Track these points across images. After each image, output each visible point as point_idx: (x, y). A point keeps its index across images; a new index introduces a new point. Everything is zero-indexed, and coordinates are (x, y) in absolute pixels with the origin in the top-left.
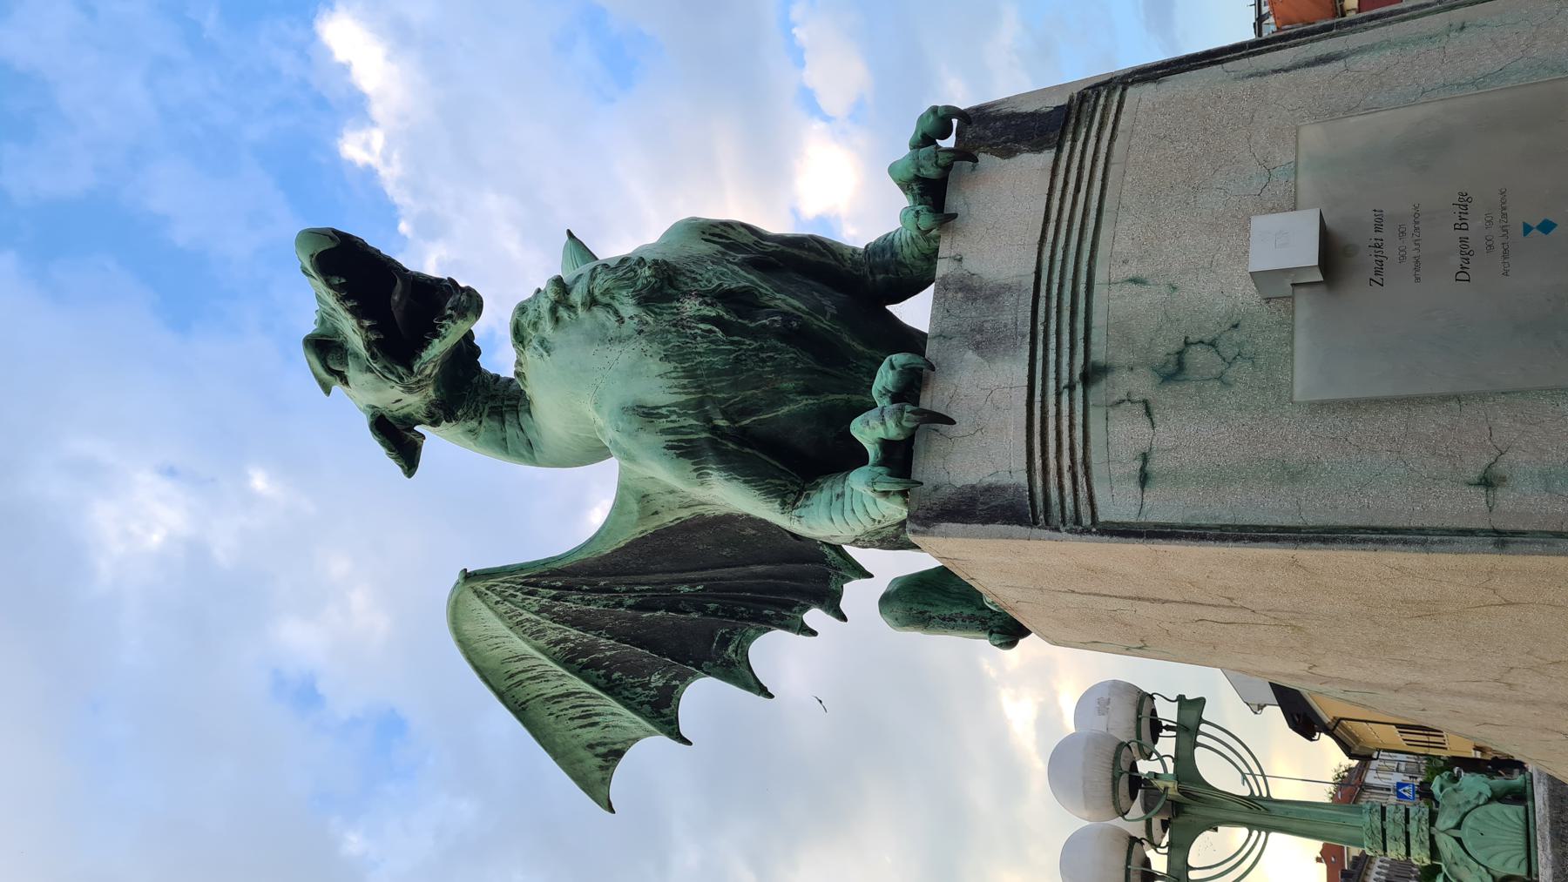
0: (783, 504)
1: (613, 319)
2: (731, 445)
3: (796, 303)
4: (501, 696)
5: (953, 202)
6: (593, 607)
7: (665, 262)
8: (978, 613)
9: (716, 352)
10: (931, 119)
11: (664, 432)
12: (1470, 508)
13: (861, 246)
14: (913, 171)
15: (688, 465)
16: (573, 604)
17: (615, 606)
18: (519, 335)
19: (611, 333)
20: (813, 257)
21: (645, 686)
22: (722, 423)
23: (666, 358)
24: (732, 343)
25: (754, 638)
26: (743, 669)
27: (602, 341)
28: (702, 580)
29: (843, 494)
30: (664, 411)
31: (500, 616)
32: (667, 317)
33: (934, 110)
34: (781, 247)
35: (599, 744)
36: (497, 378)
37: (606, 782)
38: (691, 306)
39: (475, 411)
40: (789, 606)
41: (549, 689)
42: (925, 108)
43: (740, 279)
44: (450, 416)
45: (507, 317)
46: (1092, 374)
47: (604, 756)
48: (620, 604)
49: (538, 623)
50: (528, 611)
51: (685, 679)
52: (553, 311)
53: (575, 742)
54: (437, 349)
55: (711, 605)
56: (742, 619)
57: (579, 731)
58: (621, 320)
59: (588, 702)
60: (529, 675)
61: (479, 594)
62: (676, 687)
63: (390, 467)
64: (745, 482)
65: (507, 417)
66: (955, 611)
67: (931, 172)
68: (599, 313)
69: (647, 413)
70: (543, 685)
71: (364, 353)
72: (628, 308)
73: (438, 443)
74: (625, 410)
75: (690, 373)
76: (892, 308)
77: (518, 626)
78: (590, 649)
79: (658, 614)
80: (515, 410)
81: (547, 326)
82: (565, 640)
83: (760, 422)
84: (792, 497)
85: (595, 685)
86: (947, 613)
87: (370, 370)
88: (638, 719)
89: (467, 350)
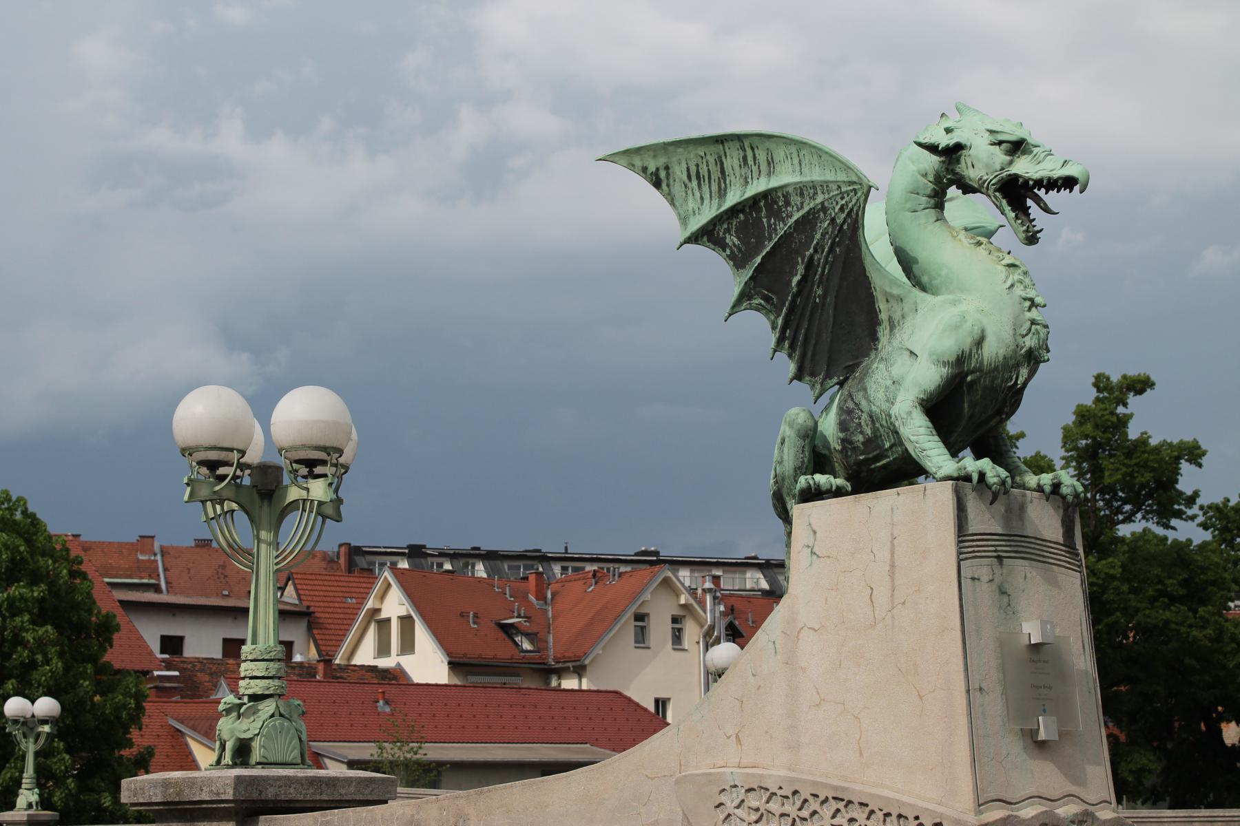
0: (922, 400)
4: (739, 138)
12: (974, 685)
15: (953, 359)
21: (728, 231)
22: (969, 378)
23: (1005, 358)
28: (823, 304)
37: (631, 166)
40: (792, 347)
46: (999, 558)
47: (656, 173)
48: (816, 251)
51: (738, 262)
52: (1032, 300)
59: (715, 187)
61: (851, 183)
62: (724, 251)
65: (933, 201)
69: (979, 342)
70: (736, 163)
73: (932, 162)
74: (983, 331)
75: (996, 368)
78: (775, 213)
79: (801, 269)
81: (1019, 291)
82: (787, 203)
87: (1002, 169)
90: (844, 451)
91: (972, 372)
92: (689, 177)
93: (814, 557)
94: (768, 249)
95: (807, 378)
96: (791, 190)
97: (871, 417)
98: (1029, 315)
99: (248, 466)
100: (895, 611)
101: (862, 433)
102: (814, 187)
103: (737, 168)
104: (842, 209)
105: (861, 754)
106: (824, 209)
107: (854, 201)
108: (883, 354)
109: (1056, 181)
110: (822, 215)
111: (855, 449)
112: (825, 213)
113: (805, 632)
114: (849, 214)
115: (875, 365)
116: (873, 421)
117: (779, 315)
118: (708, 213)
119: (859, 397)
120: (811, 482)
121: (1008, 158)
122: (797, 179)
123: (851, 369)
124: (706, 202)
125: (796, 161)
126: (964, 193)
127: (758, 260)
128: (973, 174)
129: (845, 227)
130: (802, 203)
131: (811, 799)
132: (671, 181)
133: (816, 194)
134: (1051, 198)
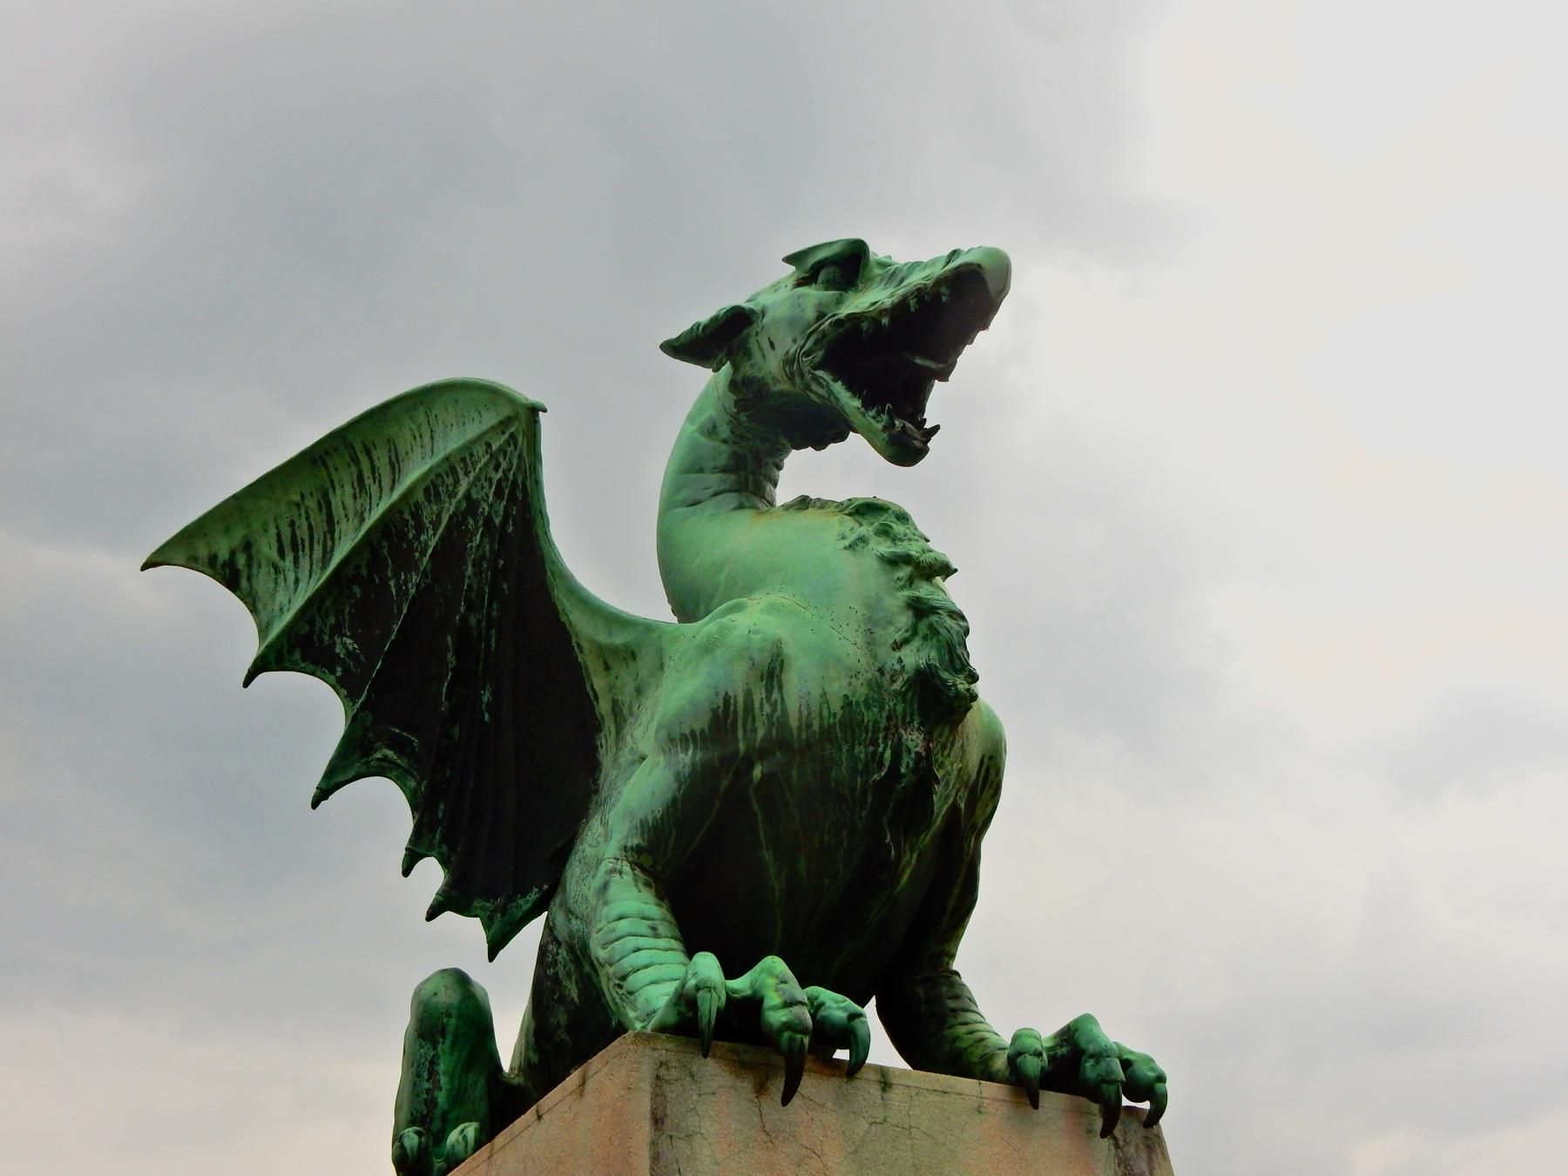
0: (638, 850)
1: (898, 637)
2: (725, 783)
3: (904, 879)
5: (1052, 1101)
6: (469, 571)
7: (969, 708)
8: (438, 1113)
9: (853, 770)
10: (1152, 1074)
11: (748, 694)
13: (956, 965)
14: (1091, 1048)
15: (702, 723)
17: (468, 599)
18: (867, 509)
19: (879, 633)
20: (952, 902)
21: (337, 630)
22: (757, 772)
23: (848, 703)
24: (864, 792)
26: (357, 767)
27: (869, 620)
29: (657, 936)
30: (775, 695)
31: (468, 447)
32: (900, 708)
33: (1161, 1079)
34: (967, 859)
35: (250, 558)
36: (780, 468)
37: (192, 563)
38: (914, 739)
39: (742, 437)
40: (445, 839)
41: (343, 497)
42: (1163, 1065)
43: (940, 807)
44: (741, 405)
45: (885, 496)
47: (231, 563)
48: (470, 607)
49: (452, 495)
50: (472, 485)
51: (347, 686)
52: (907, 559)
53: (257, 525)
54: (850, 403)
55: (457, 730)
57: (273, 531)
58: (897, 646)
60: (367, 474)
61: (504, 424)
62: (333, 672)
63: (677, 328)
64: (674, 799)
65: (732, 477)
66: (443, 1080)
67: (1090, 1069)
68: (905, 620)
69: (772, 672)
70: (349, 491)
71: (844, 312)
72: (914, 657)
75: (827, 733)
76: (873, 1001)
77: (451, 467)
78: (405, 562)
80: (740, 488)
81: (884, 547)
82: (420, 528)
84: (647, 861)
85: (345, 562)
86: (442, 1067)
87: (821, 316)
88: (288, 616)
91: (763, 753)
97: (571, 949)
98: (907, 593)
101: (563, 1000)
103: (349, 501)
104: (499, 493)
106: (471, 504)
107: (515, 462)
108: (603, 795)
110: (471, 521)
114: (512, 498)
118: (293, 596)
122: (425, 468)
124: (302, 585)
125: (427, 439)
128: (769, 366)
129: (510, 529)
130: (439, 516)
132: (255, 567)
133: (457, 482)
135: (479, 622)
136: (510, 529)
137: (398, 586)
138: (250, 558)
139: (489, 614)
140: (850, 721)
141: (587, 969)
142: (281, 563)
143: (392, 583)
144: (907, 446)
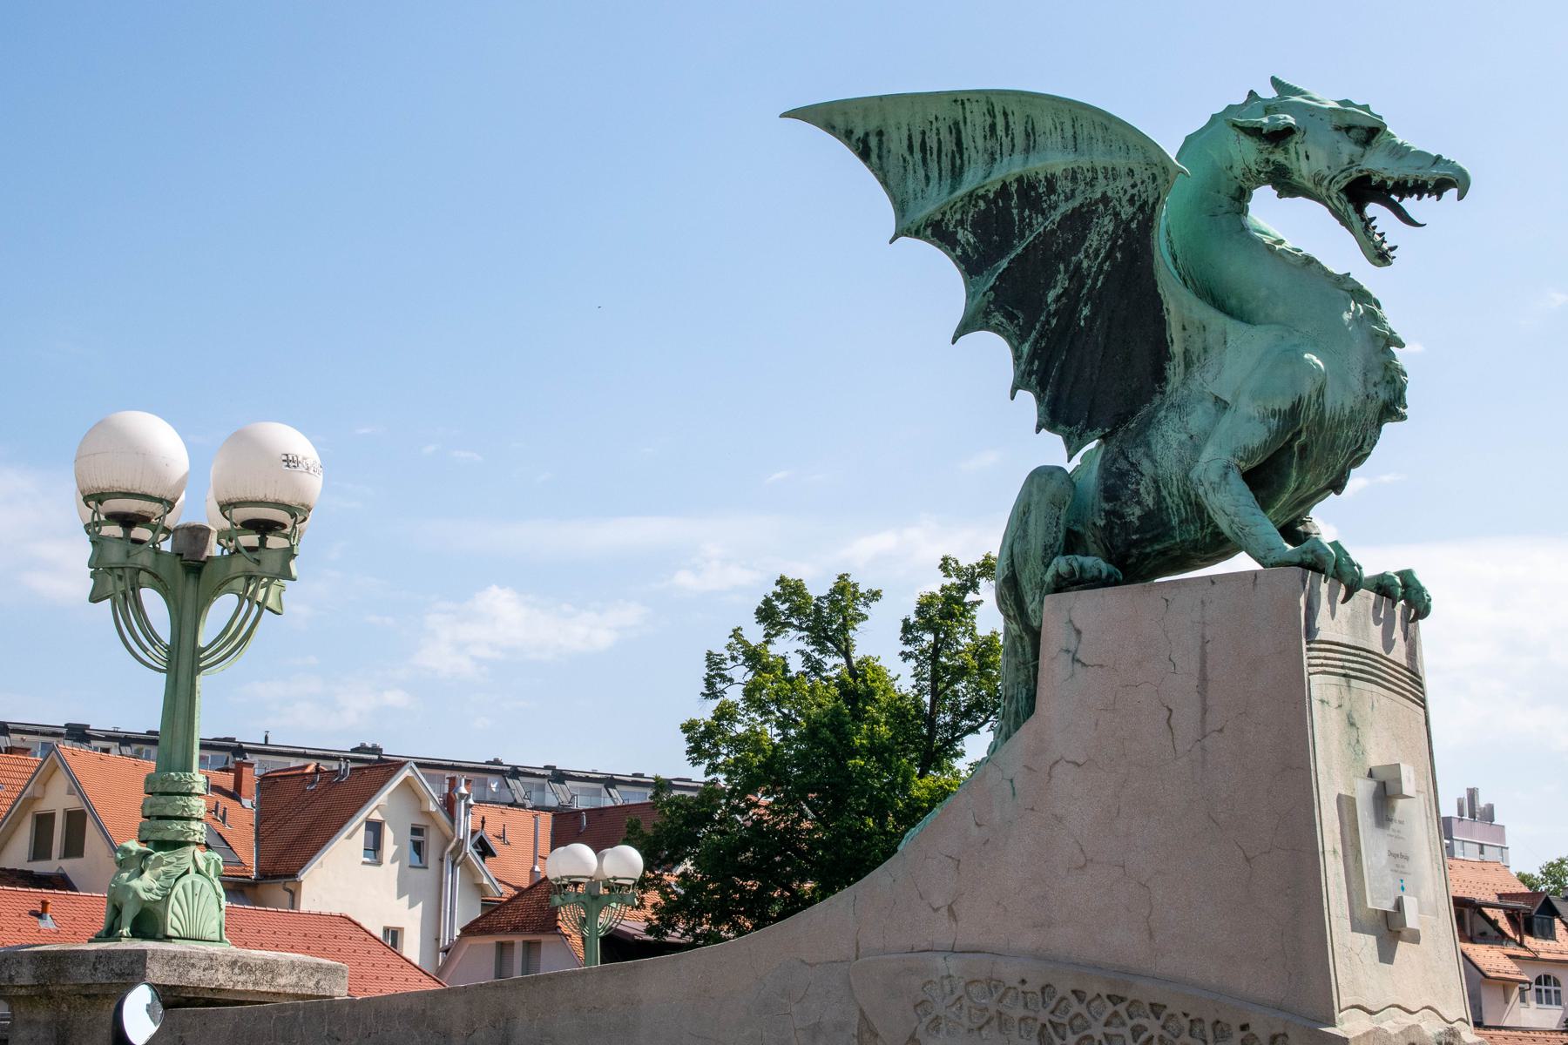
16: (1108, 224)
25: (1011, 344)
35: (880, 142)
37: (830, 128)
47: (864, 141)
49: (1091, 184)
51: (971, 267)
53: (892, 122)
56: (1036, 341)
70: (979, 134)
75: (1340, 423)
79: (1062, 282)
83: (1292, 457)
87: (1352, 162)
89: (1286, 185)
90: (1109, 526)
92: (910, 148)
93: (1078, 666)
94: (1019, 250)
95: (1061, 427)
96: (1058, 173)
97: (1155, 482)
99: (167, 530)
100: (1207, 742)
101: (1139, 503)
102: (1094, 170)
103: (980, 142)
104: (1131, 201)
105: (1151, 936)
106: (1105, 199)
109: (1425, 183)
110: (1101, 207)
111: (1126, 526)
112: (1106, 206)
113: (1058, 769)
114: (1141, 208)
115: (1163, 413)
116: (1158, 489)
117: (1023, 340)
119: (1137, 455)
120: (1075, 564)
121: (1358, 150)
123: (1122, 419)
124: (934, 182)
125: (1069, 133)
126: (1280, 196)
127: (1004, 264)
130: (1073, 191)
131: (1073, 999)
132: (885, 153)
134: (1410, 204)
135: (1090, 267)
136: (1134, 225)
137: (1022, 219)
138: (880, 142)
139: (1101, 265)
140: (1351, 421)
141: (1164, 493)
142: (908, 158)
143: (1015, 211)
144: (1381, 256)
